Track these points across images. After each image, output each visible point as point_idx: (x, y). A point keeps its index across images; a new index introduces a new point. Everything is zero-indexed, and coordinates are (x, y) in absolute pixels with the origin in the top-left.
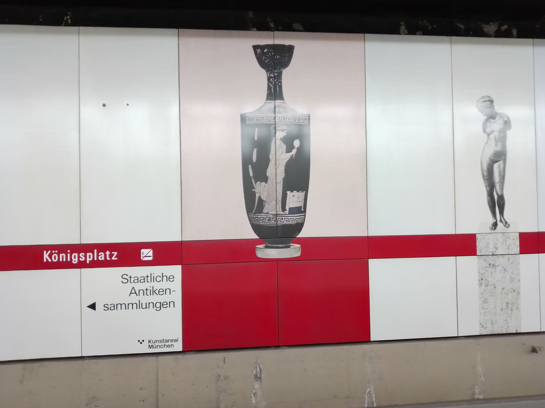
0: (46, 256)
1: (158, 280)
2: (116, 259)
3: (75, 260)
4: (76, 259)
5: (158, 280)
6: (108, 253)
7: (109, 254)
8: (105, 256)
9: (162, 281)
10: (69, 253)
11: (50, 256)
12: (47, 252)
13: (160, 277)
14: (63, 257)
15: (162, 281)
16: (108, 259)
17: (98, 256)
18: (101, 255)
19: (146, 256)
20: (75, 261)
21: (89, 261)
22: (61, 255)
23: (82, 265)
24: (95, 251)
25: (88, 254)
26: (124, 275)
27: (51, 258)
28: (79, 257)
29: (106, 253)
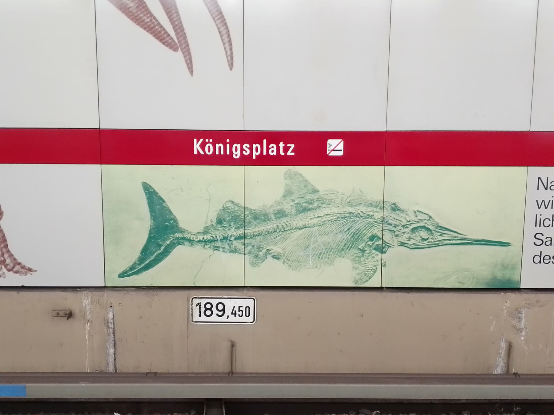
0: (197, 146)
1: (546, 225)
2: (293, 154)
3: (236, 153)
4: (239, 153)
5: (546, 225)
6: (282, 145)
7: (283, 147)
8: (278, 149)
9: (552, 226)
10: (228, 143)
11: (203, 146)
12: (197, 142)
13: (550, 220)
14: (220, 147)
15: (552, 226)
16: (282, 153)
17: (268, 149)
18: (273, 147)
19: (335, 149)
20: (237, 155)
21: (256, 156)
22: (217, 146)
23: (246, 161)
24: (265, 141)
25: (254, 146)
26: (546, 227)
27: (203, 149)
28: (242, 150)
29: (279, 145)
